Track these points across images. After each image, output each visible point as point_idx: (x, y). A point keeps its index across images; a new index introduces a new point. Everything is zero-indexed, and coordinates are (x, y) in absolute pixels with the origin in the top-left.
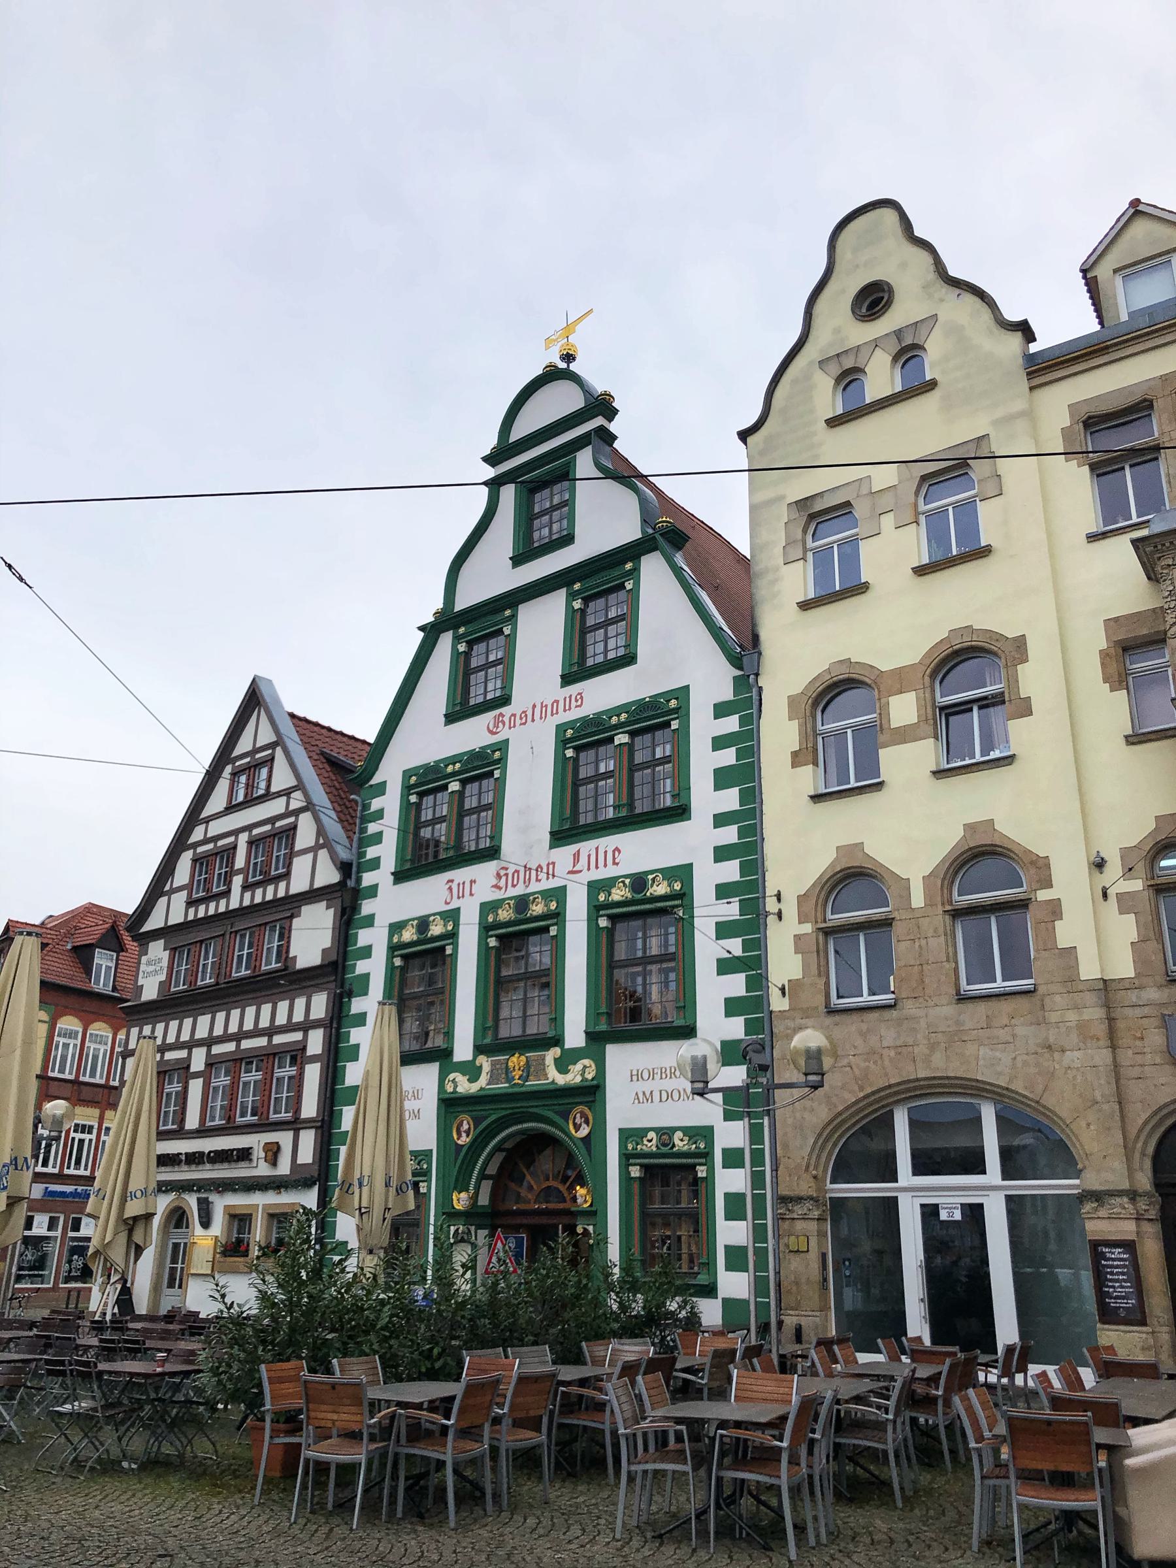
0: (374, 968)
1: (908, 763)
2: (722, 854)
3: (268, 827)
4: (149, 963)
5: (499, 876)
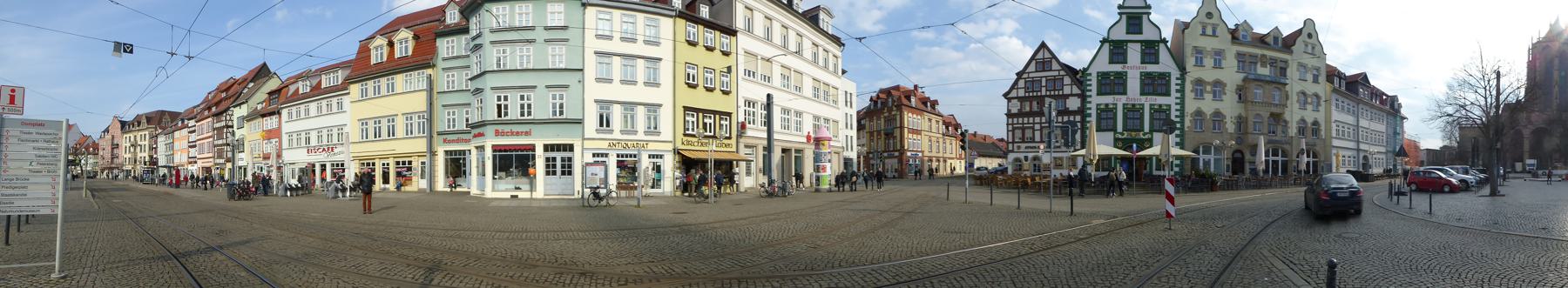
0: (1093, 112)
1: (1208, 97)
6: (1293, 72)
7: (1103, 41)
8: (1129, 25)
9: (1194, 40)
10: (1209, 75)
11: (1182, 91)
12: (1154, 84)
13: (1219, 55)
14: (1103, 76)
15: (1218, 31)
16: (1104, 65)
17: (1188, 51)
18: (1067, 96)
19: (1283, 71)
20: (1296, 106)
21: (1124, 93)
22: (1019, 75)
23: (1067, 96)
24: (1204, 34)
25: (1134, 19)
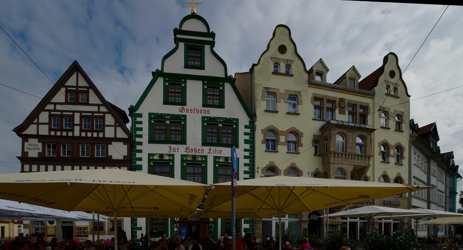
0: (145, 163)
1: (282, 149)
2: (245, 157)
3: (91, 114)
4: (29, 145)
5: (186, 149)
6: (376, 120)
7: (157, 74)
8: (187, 58)
9: (265, 80)
10: (282, 122)
11: (251, 142)
12: (219, 132)
13: (294, 98)
14: (157, 120)
15: (294, 70)
16: (156, 104)
17: (259, 93)
18: (110, 141)
19: (364, 118)
20: (378, 158)
21: (183, 142)
22: (40, 108)
23: (110, 141)
24: (275, 73)
25: (196, 43)
